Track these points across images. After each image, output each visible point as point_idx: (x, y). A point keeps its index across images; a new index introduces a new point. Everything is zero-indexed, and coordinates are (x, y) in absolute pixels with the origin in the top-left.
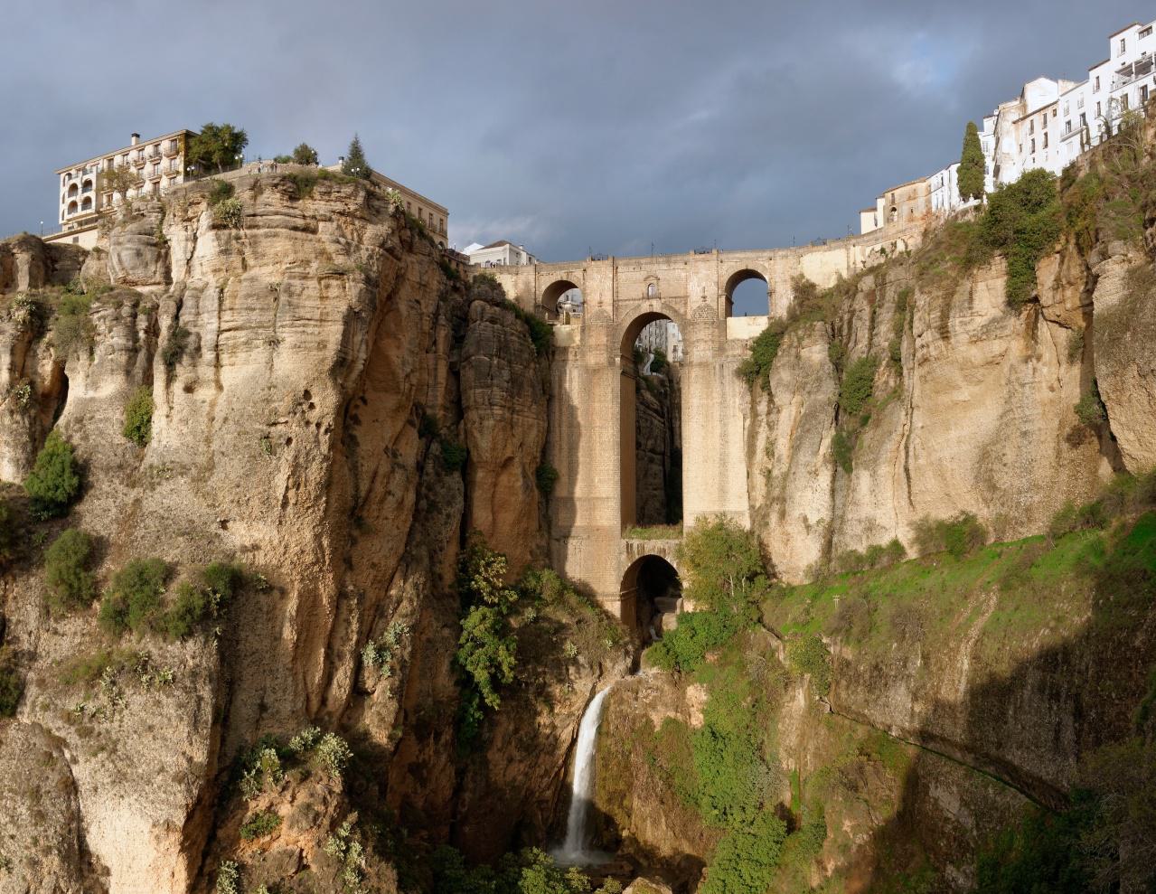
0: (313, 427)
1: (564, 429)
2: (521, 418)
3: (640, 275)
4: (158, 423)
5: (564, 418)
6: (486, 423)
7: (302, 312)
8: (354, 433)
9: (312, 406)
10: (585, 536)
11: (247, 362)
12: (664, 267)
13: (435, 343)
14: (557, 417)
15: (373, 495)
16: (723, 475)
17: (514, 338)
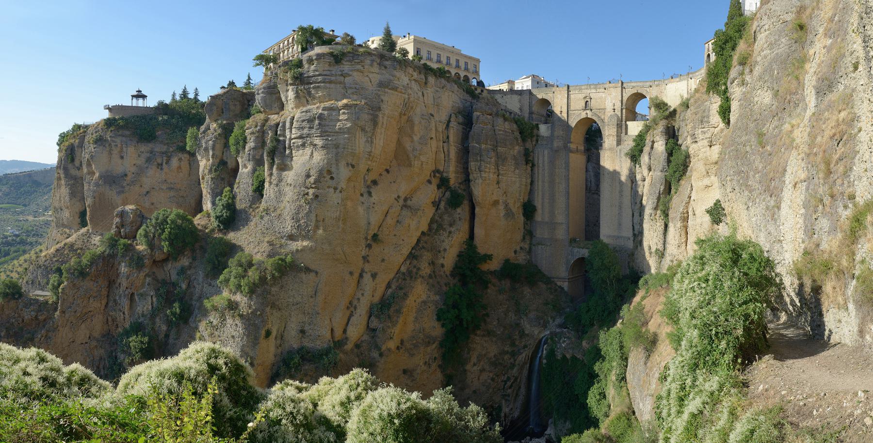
0: (332, 190)
1: (540, 183)
2: (505, 178)
3: (582, 96)
4: (266, 185)
5: (540, 177)
6: (477, 181)
7: (327, 129)
8: (371, 190)
9: (332, 178)
10: (549, 244)
11: (302, 155)
12: (594, 91)
13: (448, 137)
14: (536, 177)
15: (385, 223)
16: (620, 214)
17: (501, 132)
